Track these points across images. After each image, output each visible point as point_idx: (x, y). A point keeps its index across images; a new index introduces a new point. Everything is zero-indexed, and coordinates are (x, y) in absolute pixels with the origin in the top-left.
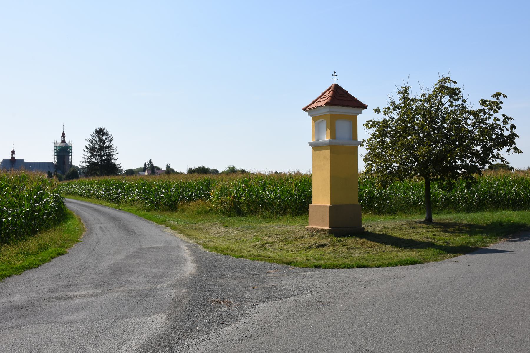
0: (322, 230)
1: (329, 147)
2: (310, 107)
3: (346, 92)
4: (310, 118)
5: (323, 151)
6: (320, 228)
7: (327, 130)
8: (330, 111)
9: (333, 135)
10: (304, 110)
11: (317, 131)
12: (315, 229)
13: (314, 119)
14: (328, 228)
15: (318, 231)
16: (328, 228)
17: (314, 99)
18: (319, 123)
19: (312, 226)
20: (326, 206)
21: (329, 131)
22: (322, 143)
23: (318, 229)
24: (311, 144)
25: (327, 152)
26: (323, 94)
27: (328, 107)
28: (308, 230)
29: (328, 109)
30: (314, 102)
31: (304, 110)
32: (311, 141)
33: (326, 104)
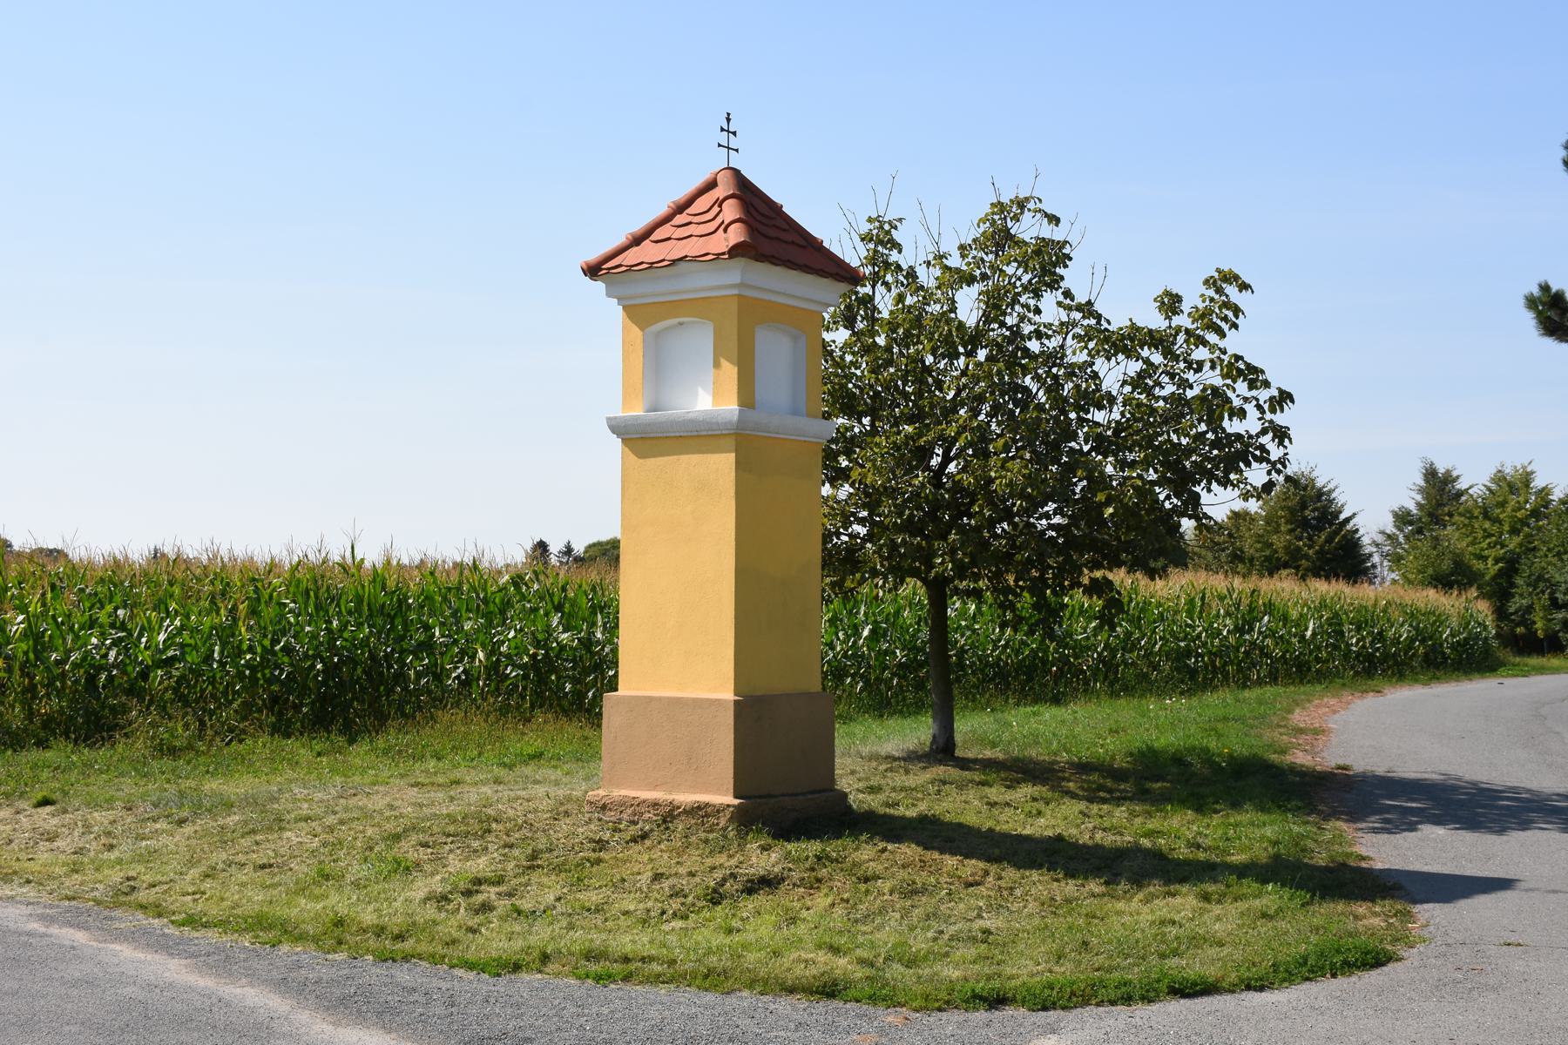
0: (698, 811)
1: (731, 442)
2: (630, 257)
3: (776, 209)
4: (613, 311)
5: (695, 458)
6: (686, 798)
7: (717, 365)
8: (741, 285)
9: (747, 397)
10: (593, 271)
11: (655, 367)
12: (655, 804)
13: (637, 313)
14: (730, 800)
15: (669, 815)
16: (730, 800)
17: (638, 225)
18: (658, 335)
19: (623, 792)
21: (730, 371)
22: (692, 421)
23: (673, 807)
24: (617, 427)
25: (722, 466)
26: (681, 208)
27: (740, 262)
28: (604, 807)
29: (734, 274)
30: (637, 240)
31: (593, 271)
32: (619, 413)
33: (736, 251)
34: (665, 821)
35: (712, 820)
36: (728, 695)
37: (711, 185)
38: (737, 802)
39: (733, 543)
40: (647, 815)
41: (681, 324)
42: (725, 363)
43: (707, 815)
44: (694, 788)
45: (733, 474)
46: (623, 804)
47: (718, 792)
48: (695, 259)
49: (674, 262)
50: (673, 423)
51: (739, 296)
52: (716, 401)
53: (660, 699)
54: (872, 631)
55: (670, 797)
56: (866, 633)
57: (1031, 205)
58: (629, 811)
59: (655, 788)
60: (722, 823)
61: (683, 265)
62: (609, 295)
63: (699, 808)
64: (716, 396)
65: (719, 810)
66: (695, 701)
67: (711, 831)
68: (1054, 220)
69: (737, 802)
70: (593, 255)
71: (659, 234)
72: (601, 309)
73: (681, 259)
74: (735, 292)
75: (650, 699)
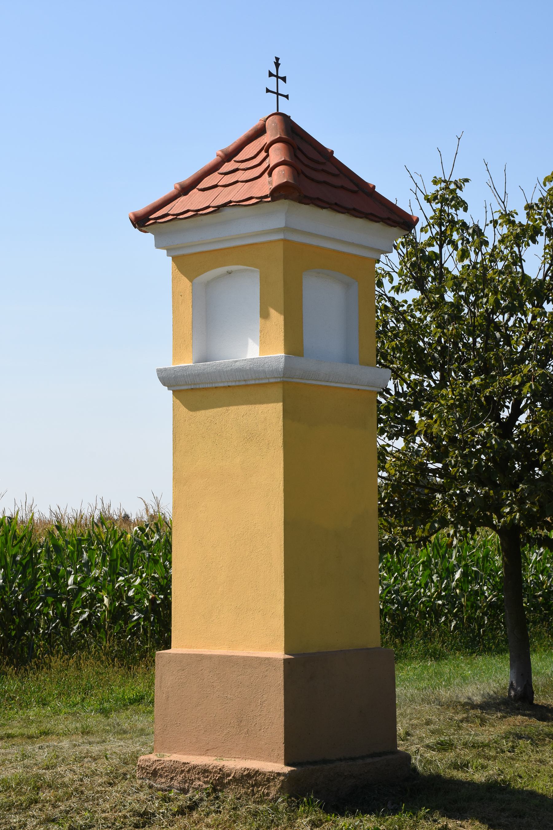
0: (249, 778)
1: (278, 391)
2: (177, 207)
3: (327, 155)
4: (163, 262)
5: (244, 409)
6: (236, 764)
7: (265, 315)
8: (286, 229)
9: (294, 343)
10: (141, 221)
11: (204, 317)
12: (205, 771)
13: (187, 264)
14: (280, 767)
15: (219, 782)
17: (186, 175)
18: (208, 284)
19: (175, 757)
20: (268, 661)
21: (277, 319)
22: (240, 370)
23: (223, 773)
24: (168, 379)
25: (269, 415)
26: (229, 156)
27: (283, 205)
28: (155, 774)
29: (279, 217)
30: (185, 190)
31: (141, 221)
32: (168, 363)
33: (278, 193)
34: (215, 790)
35: (263, 790)
37: (260, 131)
38: (287, 769)
39: (282, 495)
40: (197, 783)
41: (229, 273)
42: (273, 313)
43: (257, 784)
44: (244, 754)
45: (281, 423)
46: (174, 770)
47: (269, 758)
48: (238, 204)
49: (219, 208)
50: (220, 373)
51: (285, 240)
52: (261, 351)
56: (457, 576)
58: (180, 778)
59: (206, 752)
61: (227, 211)
62: (158, 246)
63: (249, 776)
64: (263, 344)
66: (246, 659)
69: (289, 769)
70: (141, 205)
71: (206, 182)
72: (151, 258)
73: (225, 205)
74: (281, 236)
75: (201, 658)
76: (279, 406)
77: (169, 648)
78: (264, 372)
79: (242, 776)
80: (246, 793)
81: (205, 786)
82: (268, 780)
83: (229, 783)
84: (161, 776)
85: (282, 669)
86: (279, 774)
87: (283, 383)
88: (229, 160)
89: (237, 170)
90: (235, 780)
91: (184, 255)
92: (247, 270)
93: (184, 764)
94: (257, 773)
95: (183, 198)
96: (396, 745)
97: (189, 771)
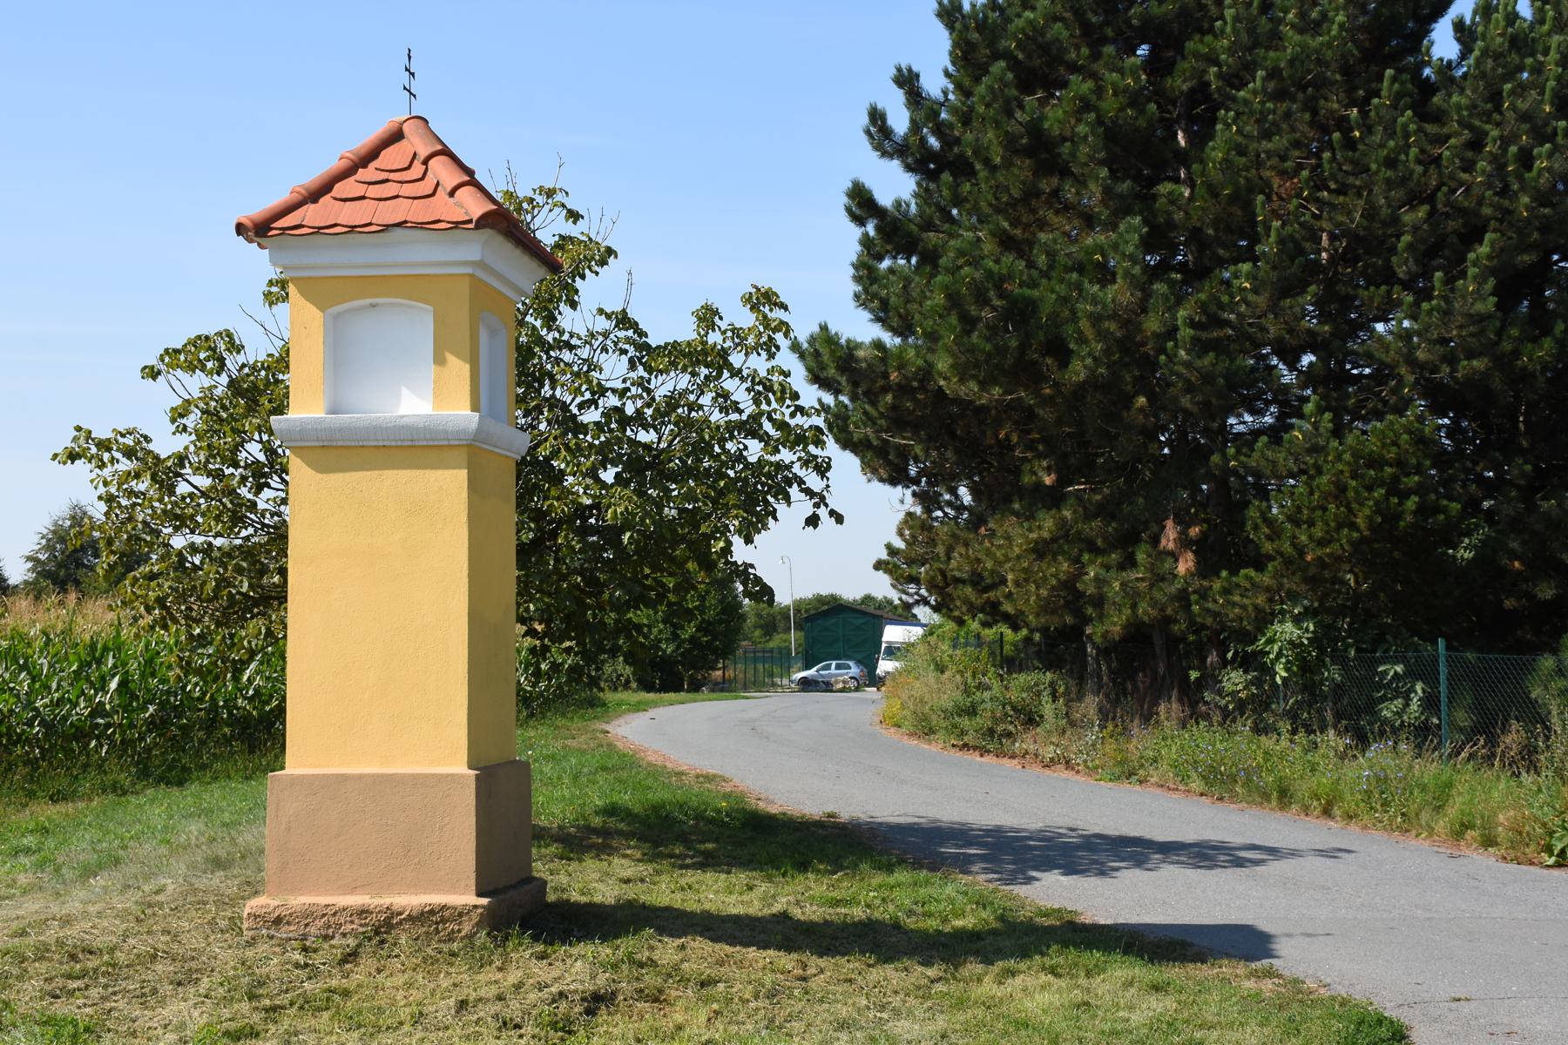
1: (462, 456)
7: (439, 360)
8: (481, 264)
12: (363, 912)
14: (471, 899)
16: (471, 899)
28: (278, 921)
30: (315, 195)
31: (258, 230)
34: (377, 933)
35: (450, 926)
36: (459, 766)
37: (396, 136)
39: (466, 580)
40: (350, 927)
41: (374, 305)
42: (452, 359)
43: (443, 921)
44: (415, 887)
46: (308, 915)
47: (452, 890)
48: (420, 226)
50: (376, 430)
51: (471, 276)
52: (436, 406)
53: (360, 777)
54: (120, 684)
55: (386, 901)
56: (113, 685)
57: (559, 197)
58: (319, 923)
59: (353, 890)
60: (467, 928)
61: (399, 232)
63: (432, 912)
64: (439, 396)
65: (461, 914)
67: (451, 940)
68: (574, 216)
69: (484, 901)
70: (257, 206)
71: (340, 189)
73: (399, 225)
74: (469, 270)
75: (343, 779)
76: (463, 474)
77: (283, 768)
78: (446, 432)
79: (422, 914)
80: (427, 933)
81: (361, 930)
82: (460, 915)
83: (400, 923)
84: (288, 923)
85: (473, 786)
86: (475, 907)
87: (469, 446)
88: (365, 166)
89: (387, 181)
90: (410, 918)
91: (310, 278)
92: (401, 305)
93: (327, 906)
94: (444, 907)
95: (311, 207)
96: (530, 868)
97: (335, 914)
